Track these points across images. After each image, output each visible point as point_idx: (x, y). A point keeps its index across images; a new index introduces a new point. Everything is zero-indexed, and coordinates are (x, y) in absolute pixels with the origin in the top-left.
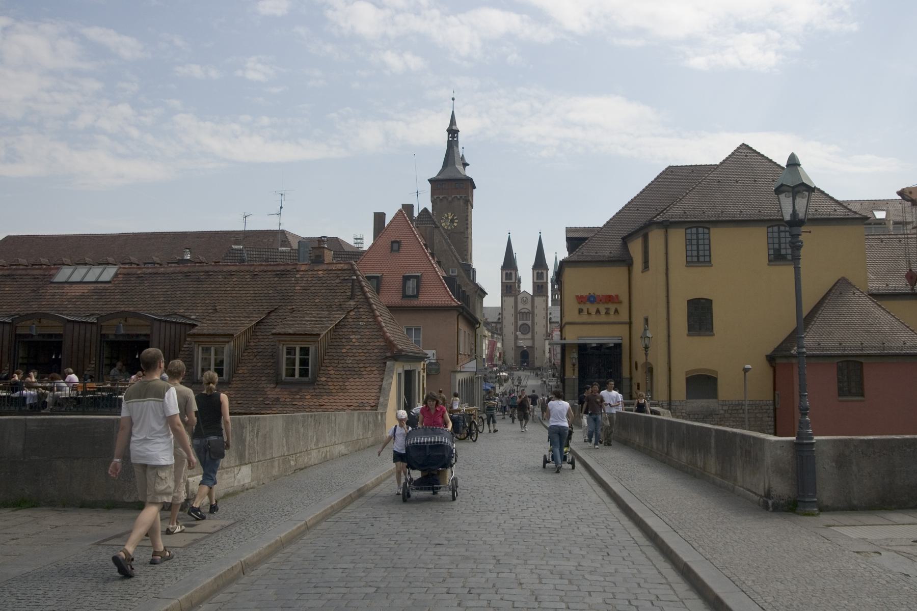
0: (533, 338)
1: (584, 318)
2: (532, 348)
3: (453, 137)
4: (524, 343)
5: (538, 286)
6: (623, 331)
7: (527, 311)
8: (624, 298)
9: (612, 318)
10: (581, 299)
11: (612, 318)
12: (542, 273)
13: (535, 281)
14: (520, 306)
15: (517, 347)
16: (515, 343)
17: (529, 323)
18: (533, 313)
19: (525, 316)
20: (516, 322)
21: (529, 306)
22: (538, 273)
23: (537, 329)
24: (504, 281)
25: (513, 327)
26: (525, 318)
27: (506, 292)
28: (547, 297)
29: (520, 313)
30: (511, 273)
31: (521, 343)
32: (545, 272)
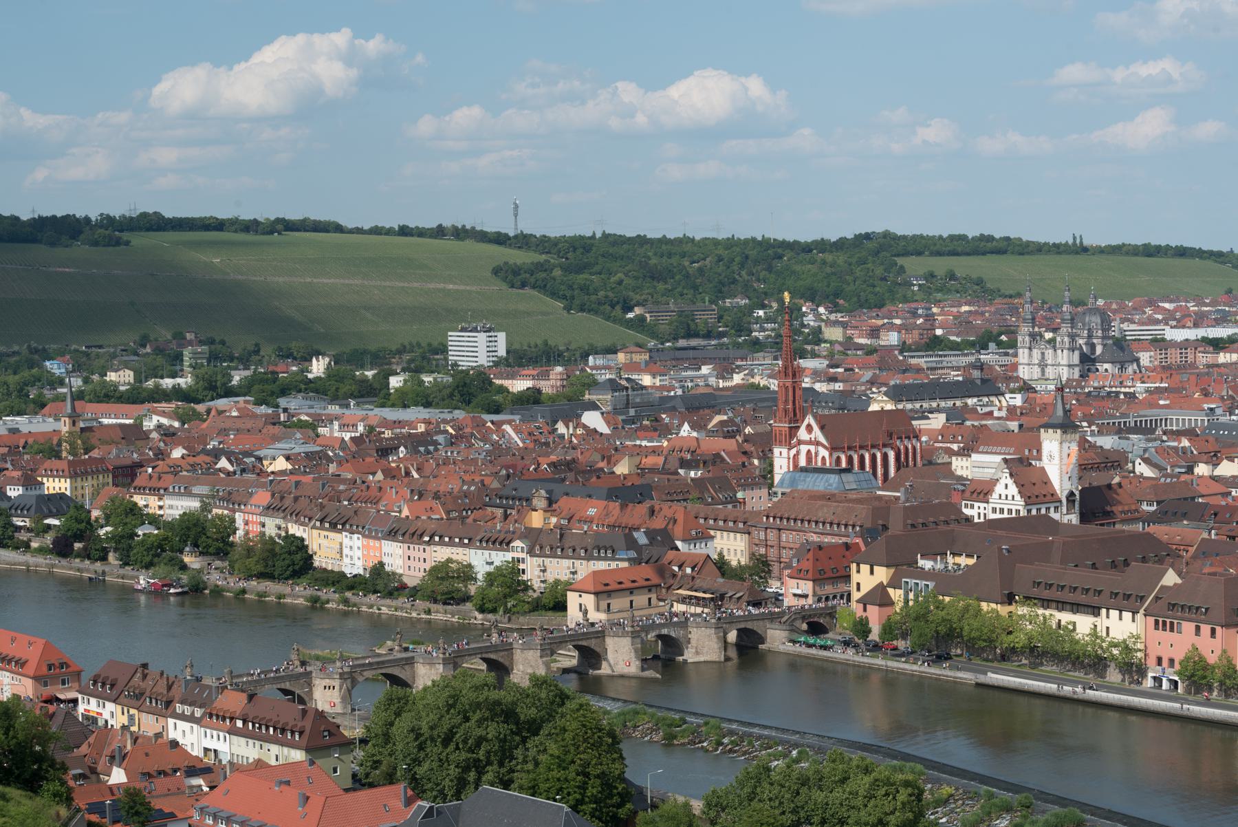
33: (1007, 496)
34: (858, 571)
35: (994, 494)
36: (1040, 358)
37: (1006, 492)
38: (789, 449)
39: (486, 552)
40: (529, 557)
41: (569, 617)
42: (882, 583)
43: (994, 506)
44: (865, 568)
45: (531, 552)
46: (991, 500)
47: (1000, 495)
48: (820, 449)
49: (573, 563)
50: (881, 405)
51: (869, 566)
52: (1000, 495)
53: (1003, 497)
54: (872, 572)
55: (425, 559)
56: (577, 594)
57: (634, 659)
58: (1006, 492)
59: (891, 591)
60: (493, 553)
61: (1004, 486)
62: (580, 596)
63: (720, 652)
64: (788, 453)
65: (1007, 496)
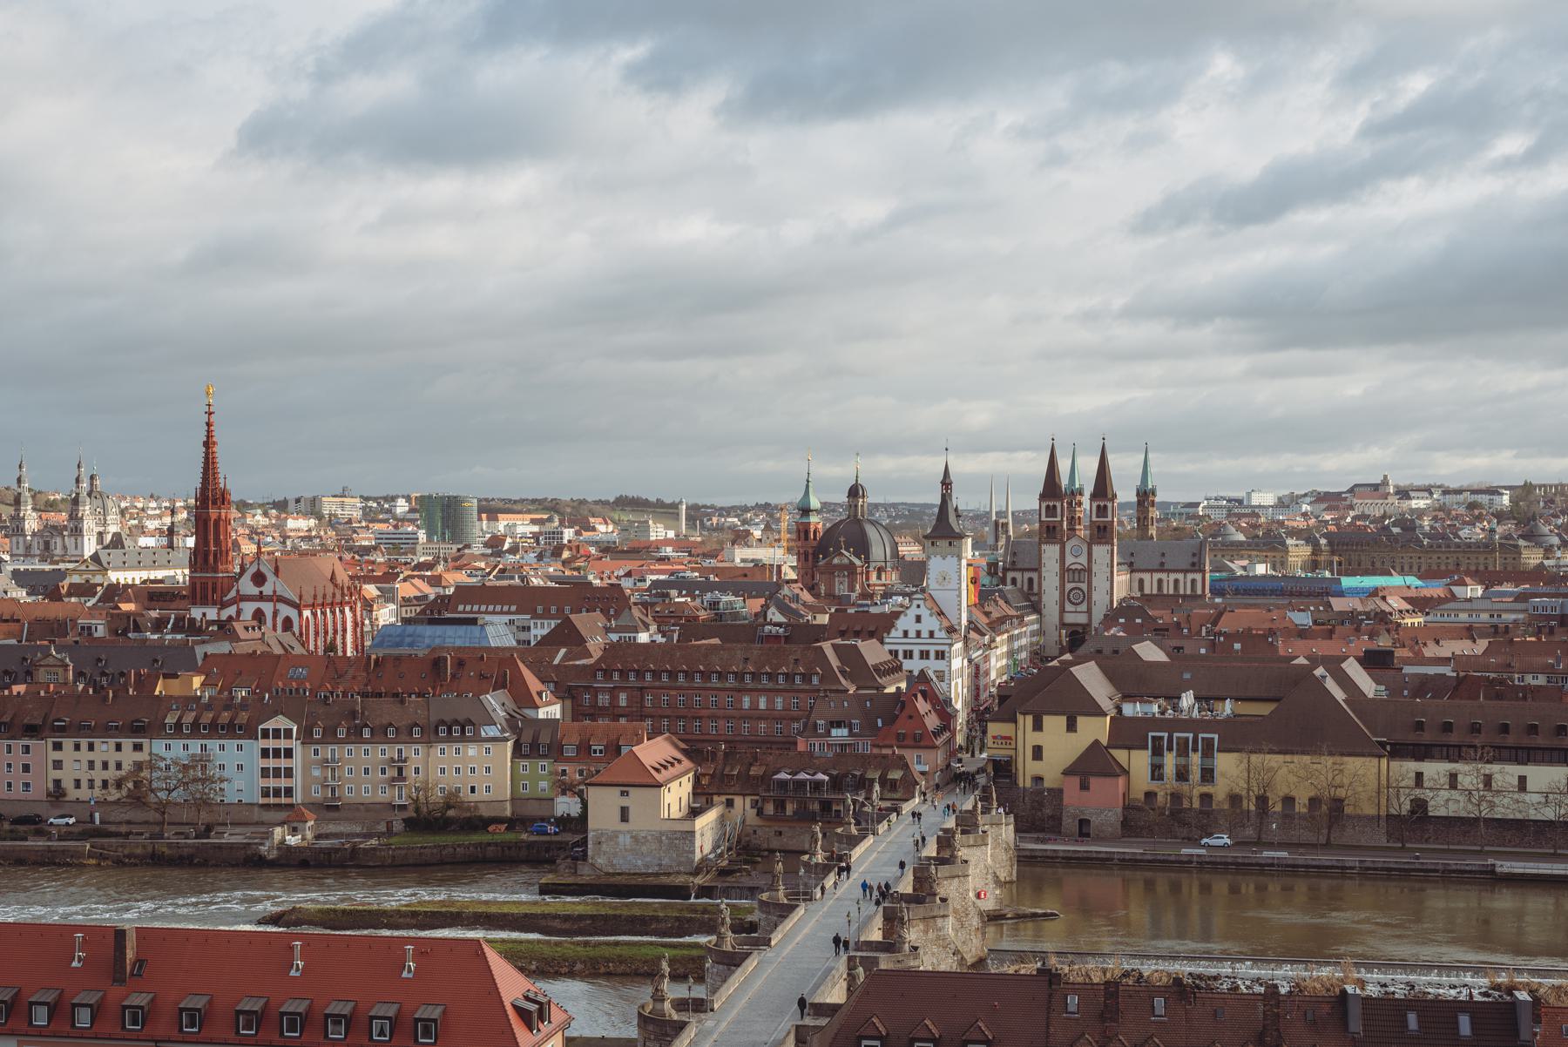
0: (1089, 611)
1: (996, 746)
2: (1089, 625)
3: (947, 489)
4: (1076, 617)
5: (1099, 527)
6: (1013, 752)
7: (1079, 567)
8: (1014, 738)
9: (1008, 746)
10: (994, 737)
11: (1008, 746)
12: (1105, 507)
13: (1094, 519)
14: (1069, 560)
15: (1063, 625)
16: (1061, 618)
17: (1084, 586)
18: (1089, 570)
19: (1076, 575)
20: (1062, 585)
21: (1083, 560)
22: (1098, 507)
23: (1095, 596)
24: (1043, 518)
25: (1057, 594)
26: (1076, 579)
27: (1048, 537)
28: (1113, 545)
29: (1069, 570)
30: (1055, 507)
31: (1069, 618)
32: (1109, 505)
33: (918, 634)
34: (1038, 726)
35: (893, 631)
36: (42, 547)
37: (918, 627)
38: (220, 609)
39: (195, 746)
40: (299, 748)
41: (591, 835)
42: (1097, 742)
43: (894, 647)
44: (1054, 723)
45: (306, 737)
46: (887, 640)
47: (906, 634)
48: (280, 606)
49: (400, 751)
50: (84, 576)
51: (1064, 719)
52: (906, 634)
53: (912, 634)
54: (1071, 727)
55: (26, 768)
56: (617, 790)
57: (992, 886)
58: (918, 627)
59: (1120, 755)
60: (213, 744)
61: (914, 620)
62: (622, 793)
63: (1011, 866)
64: (218, 614)
65: (918, 634)
